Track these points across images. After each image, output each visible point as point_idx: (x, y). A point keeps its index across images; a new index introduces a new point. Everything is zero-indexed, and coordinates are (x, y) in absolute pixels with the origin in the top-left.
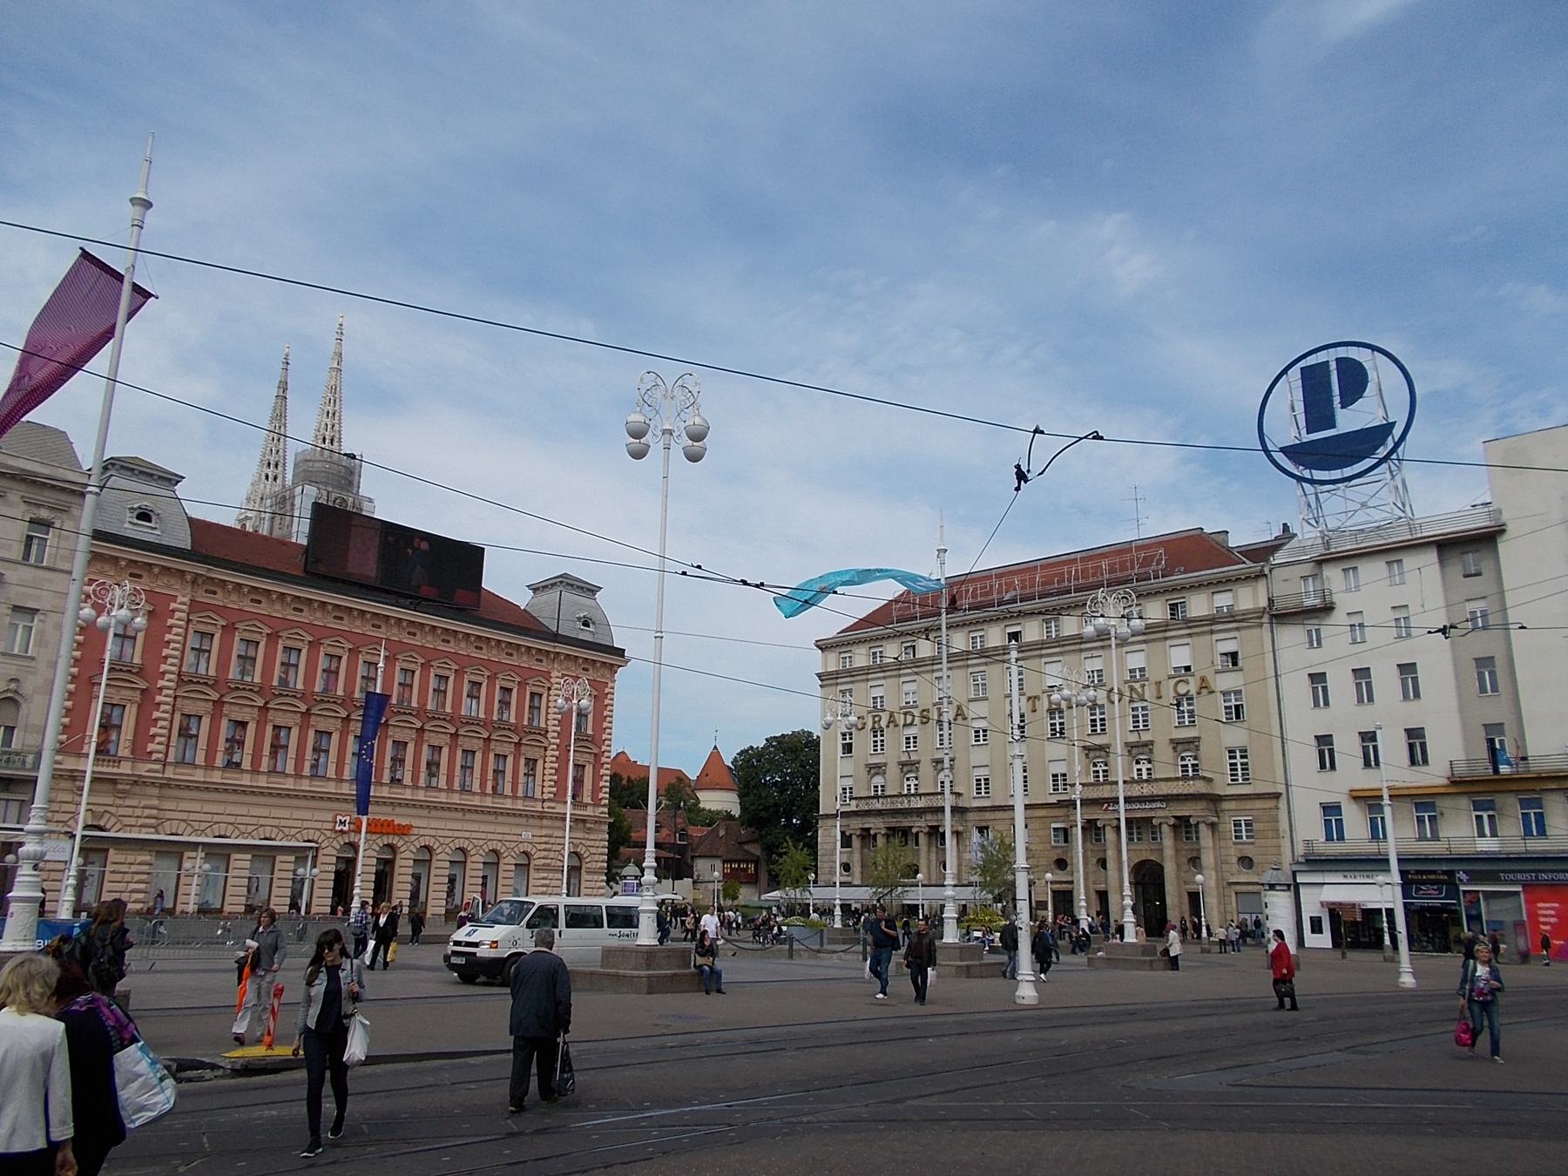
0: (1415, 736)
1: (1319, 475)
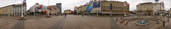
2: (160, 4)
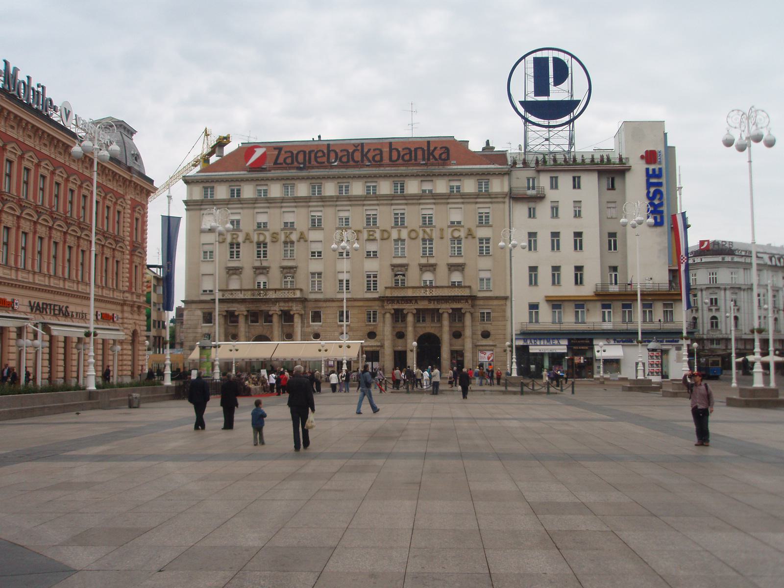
1: (553, 122)
2: (611, 172)
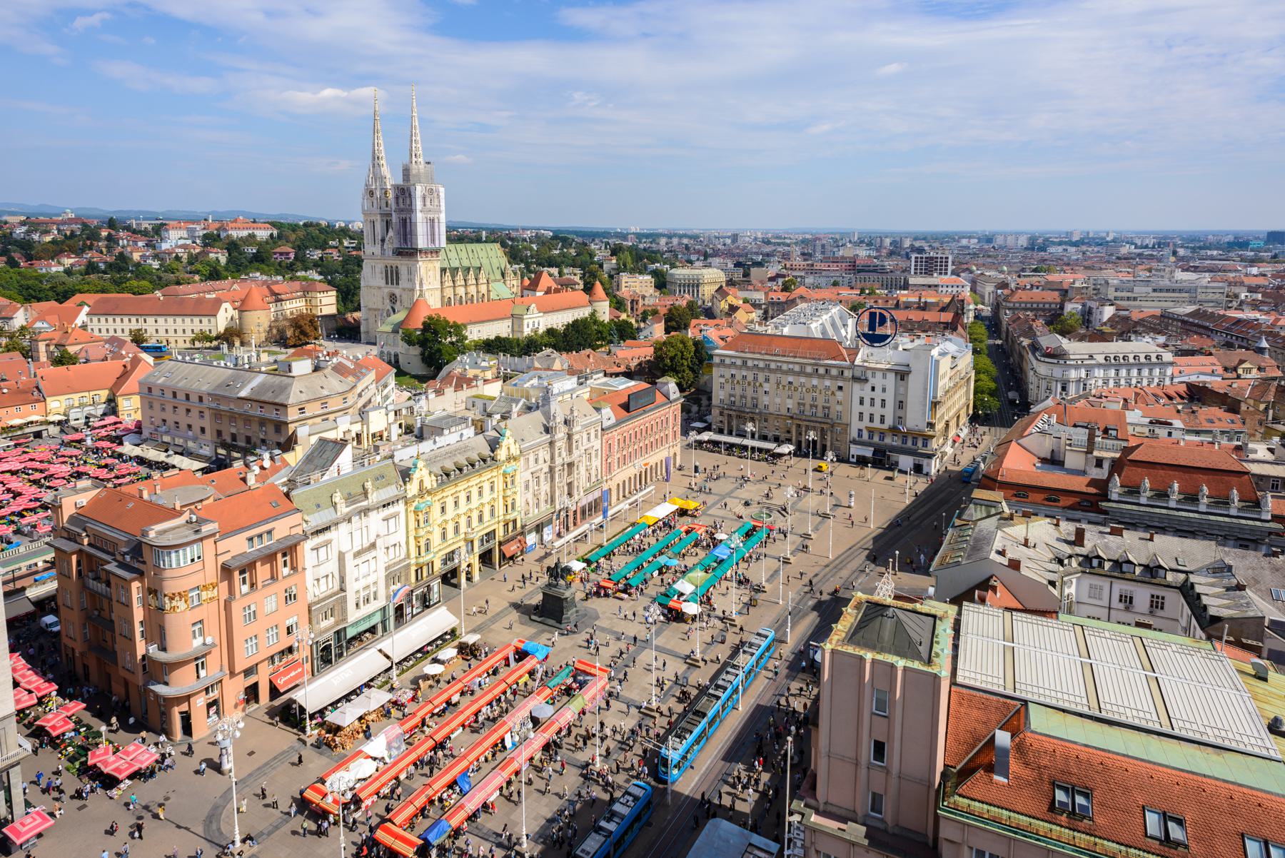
0: (882, 417)
